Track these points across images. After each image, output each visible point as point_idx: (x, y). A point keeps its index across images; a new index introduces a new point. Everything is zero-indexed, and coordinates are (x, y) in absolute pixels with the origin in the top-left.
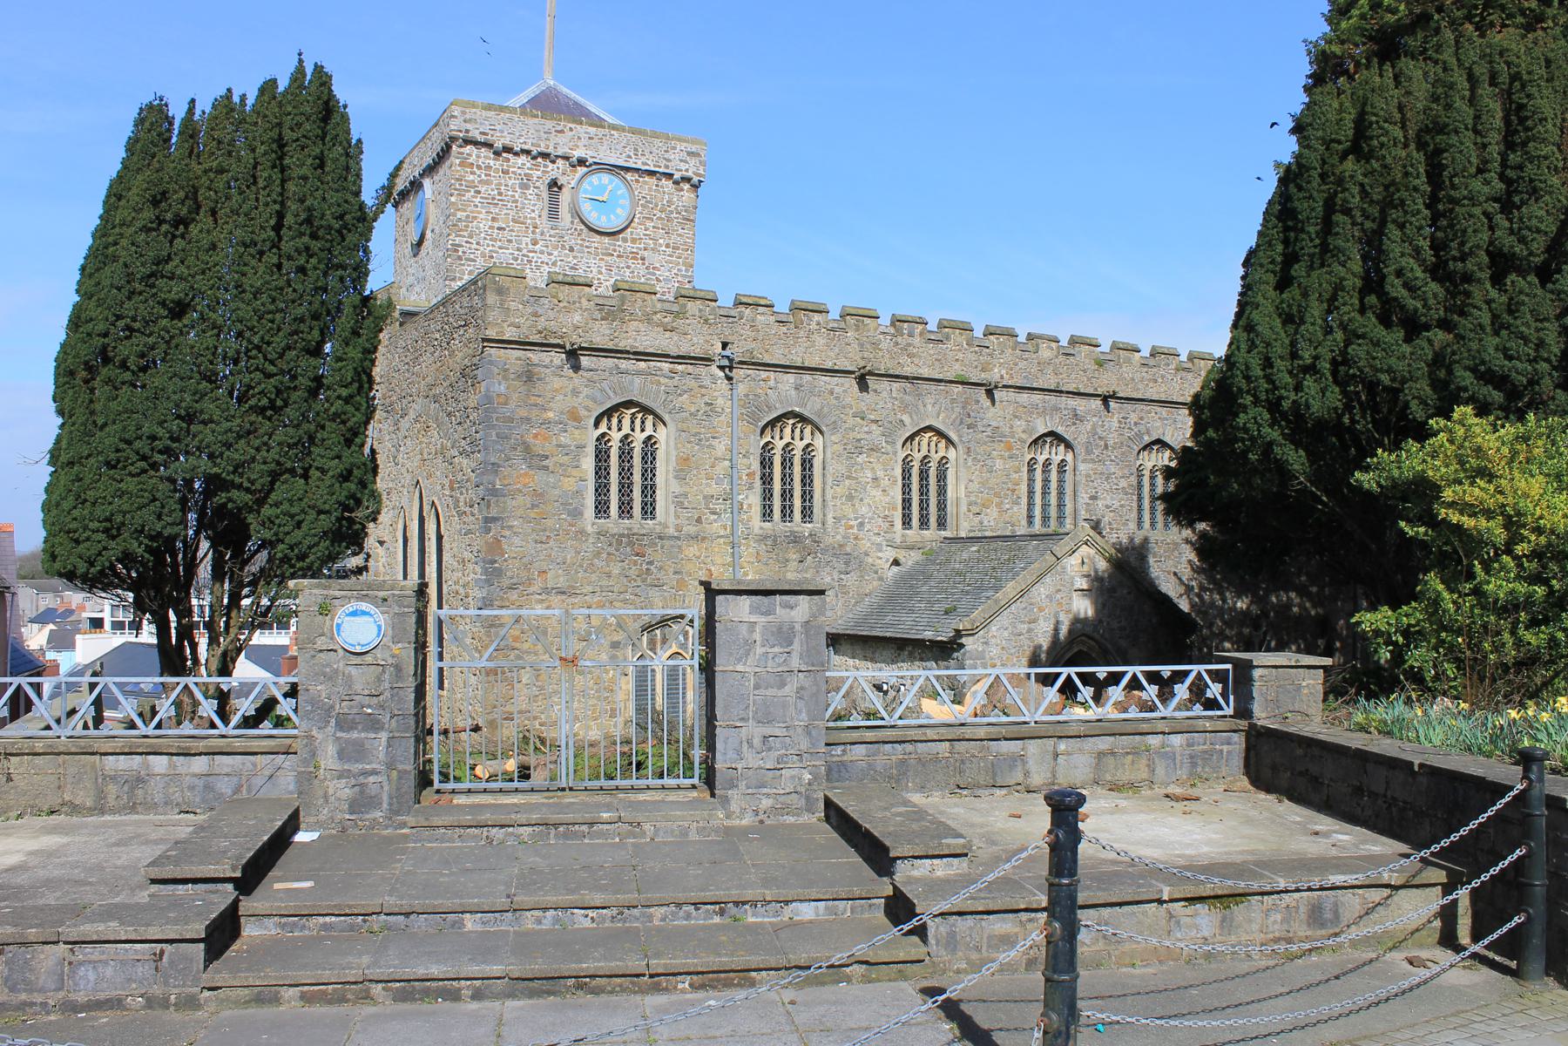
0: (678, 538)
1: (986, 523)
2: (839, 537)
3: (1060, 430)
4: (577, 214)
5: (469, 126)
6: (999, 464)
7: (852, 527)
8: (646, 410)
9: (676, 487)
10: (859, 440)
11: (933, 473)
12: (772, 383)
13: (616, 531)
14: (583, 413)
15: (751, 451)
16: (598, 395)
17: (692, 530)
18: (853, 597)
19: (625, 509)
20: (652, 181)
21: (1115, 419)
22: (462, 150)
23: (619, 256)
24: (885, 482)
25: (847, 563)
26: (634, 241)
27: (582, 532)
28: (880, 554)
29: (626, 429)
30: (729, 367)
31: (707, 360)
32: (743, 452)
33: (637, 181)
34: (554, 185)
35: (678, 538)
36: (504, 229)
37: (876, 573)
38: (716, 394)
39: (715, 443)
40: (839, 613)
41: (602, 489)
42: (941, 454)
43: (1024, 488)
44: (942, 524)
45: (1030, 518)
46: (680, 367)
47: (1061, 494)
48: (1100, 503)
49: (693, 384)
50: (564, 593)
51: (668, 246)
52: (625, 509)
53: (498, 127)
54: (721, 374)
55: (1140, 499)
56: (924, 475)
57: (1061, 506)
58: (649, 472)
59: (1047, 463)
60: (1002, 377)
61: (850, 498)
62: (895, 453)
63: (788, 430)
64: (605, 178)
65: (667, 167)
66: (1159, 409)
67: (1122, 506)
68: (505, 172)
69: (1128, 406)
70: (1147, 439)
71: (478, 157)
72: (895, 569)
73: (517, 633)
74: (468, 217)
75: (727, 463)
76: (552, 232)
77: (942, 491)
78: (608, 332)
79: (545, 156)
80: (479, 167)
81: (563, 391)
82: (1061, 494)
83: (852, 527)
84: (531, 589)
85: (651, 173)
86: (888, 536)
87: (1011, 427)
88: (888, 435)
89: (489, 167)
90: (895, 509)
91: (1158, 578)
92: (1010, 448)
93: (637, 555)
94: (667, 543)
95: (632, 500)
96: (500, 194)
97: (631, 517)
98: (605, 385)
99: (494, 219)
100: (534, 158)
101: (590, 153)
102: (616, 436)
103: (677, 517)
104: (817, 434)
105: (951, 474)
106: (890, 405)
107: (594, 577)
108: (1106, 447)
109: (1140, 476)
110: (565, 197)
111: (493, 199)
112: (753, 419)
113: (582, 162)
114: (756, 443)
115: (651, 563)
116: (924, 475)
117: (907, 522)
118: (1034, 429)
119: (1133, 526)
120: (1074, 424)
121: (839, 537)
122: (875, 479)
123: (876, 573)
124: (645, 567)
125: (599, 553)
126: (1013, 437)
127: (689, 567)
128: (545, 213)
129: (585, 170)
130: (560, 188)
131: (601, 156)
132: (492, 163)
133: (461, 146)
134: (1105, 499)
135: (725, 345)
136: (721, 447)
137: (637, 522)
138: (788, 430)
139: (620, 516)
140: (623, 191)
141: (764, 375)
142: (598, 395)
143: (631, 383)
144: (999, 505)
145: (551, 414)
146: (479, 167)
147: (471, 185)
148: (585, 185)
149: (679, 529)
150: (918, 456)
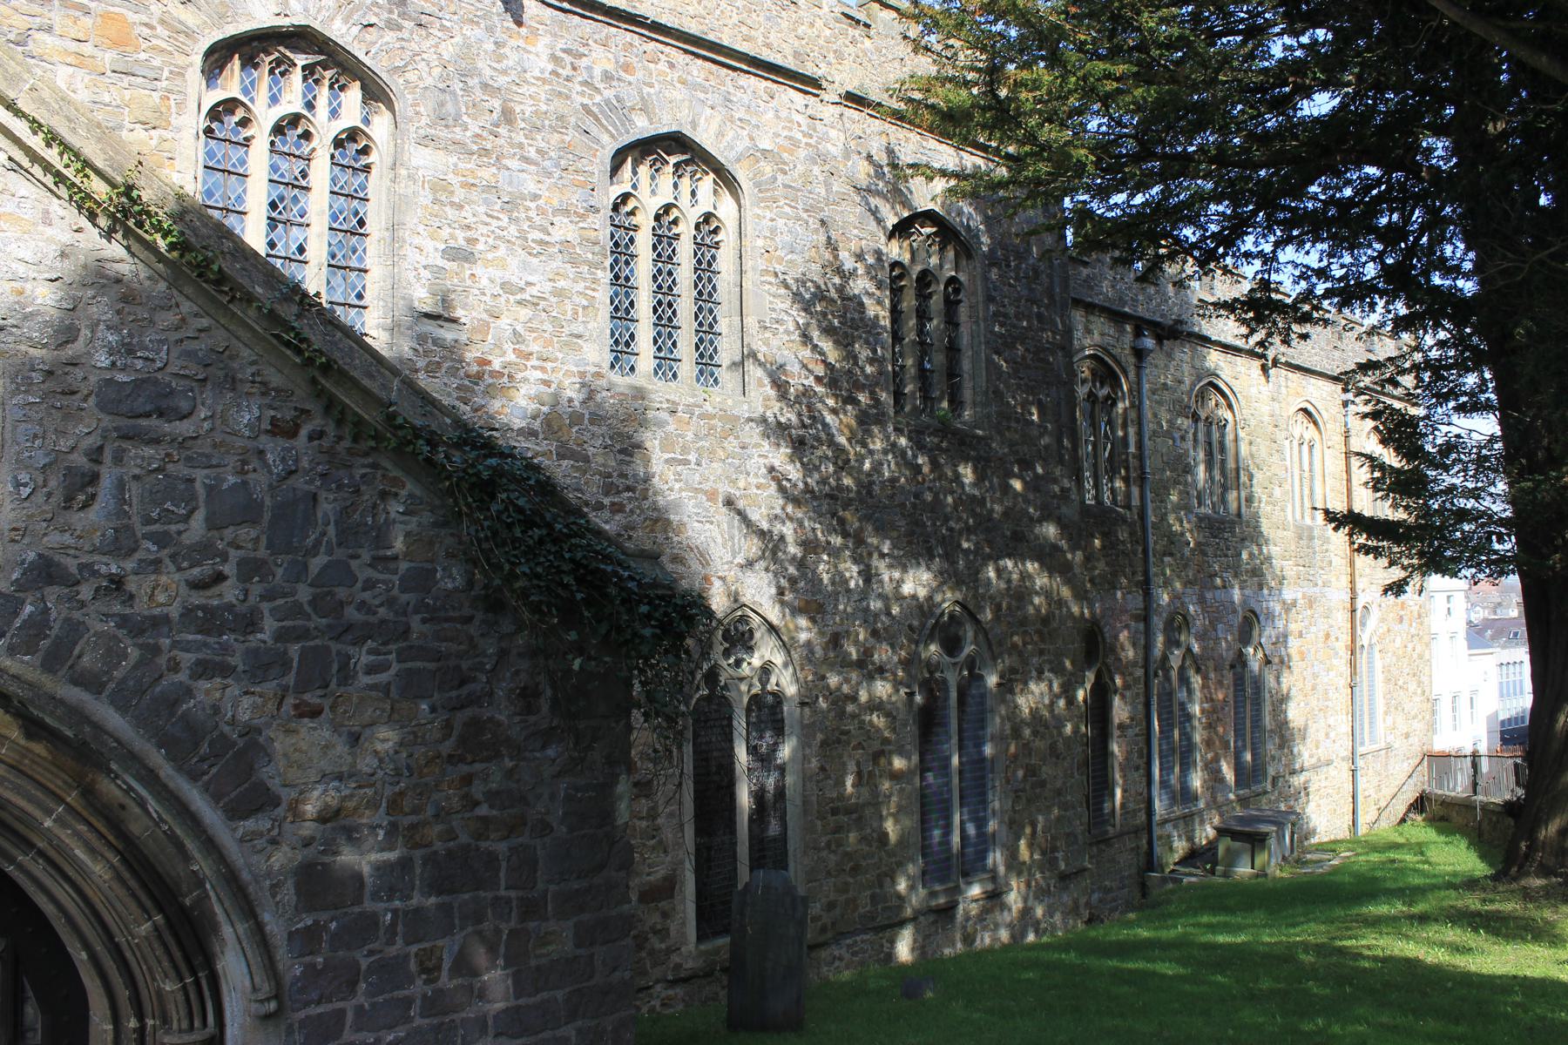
21: (542, 46)
55: (621, 281)
67: (559, 293)
70: (643, 127)
91: (677, 505)
92: (120, 43)
108: (508, 116)
119: (596, 353)
120: (393, 26)
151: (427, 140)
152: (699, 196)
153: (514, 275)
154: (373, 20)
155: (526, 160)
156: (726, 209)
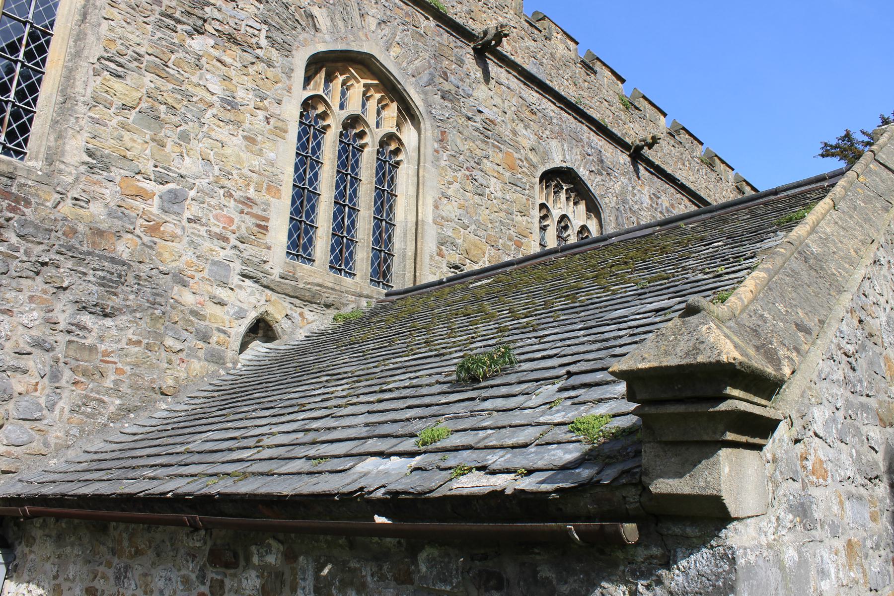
2: (96, 209)
3: (583, 172)
6: (494, 186)
7: (142, 195)
18: (116, 390)
25: (110, 284)
28: (222, 293)
37: (205, 338)
40: (55, 435)
72: (258, 348)
83: (142, 195)
86: (249, 251)
118: (545, 156)
123: (205, 338)
154: (593, 169)
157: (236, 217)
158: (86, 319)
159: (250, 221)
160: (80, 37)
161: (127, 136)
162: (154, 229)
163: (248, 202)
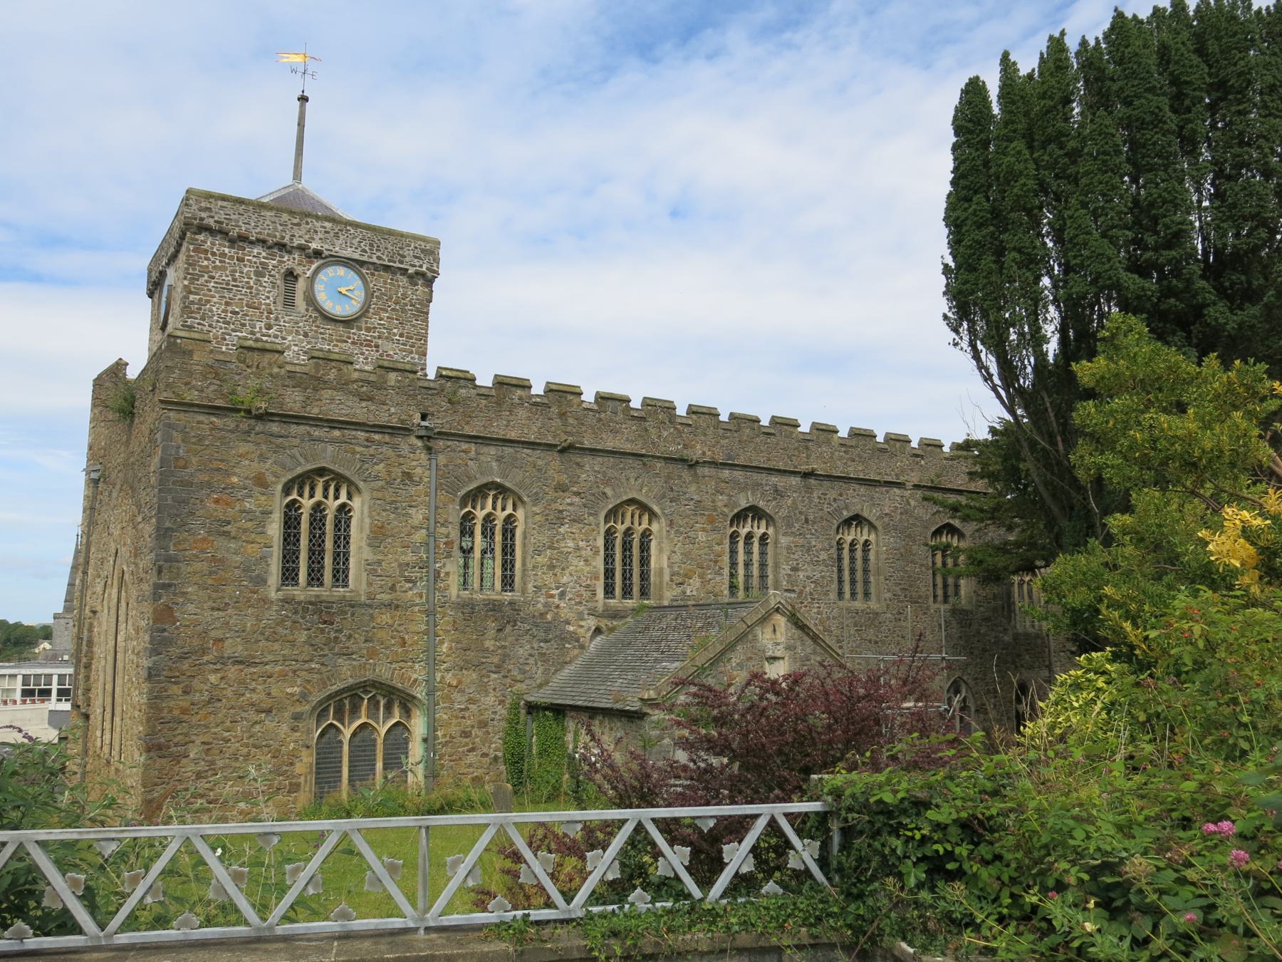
0: (370, 606)
1: (688, 593)
3: (761, 504)
4: (311, 300)
5: (204, 215)
6: (702, 537)
7: (552, 596)
8: (340, 479)
9: (368, 554)
10: (561, 512)
11: (636, 544)
12: (472, 454)
13: (302, 598)
14: (270, 478)
15: (450, 520)
16: (288, 462)
17: (385, 597)
19: (315, 577)
20: (388, 277)
22: (197, 237)
23: (353, 343)
24: (587, 553)
26: (368, 330)
27: (265, 600)
28: (582, 623)
29: (319, 496)
30: (428, 438)
31: (404, 431)
32: (442, 521)
33: (373, 274)
34: (291, 276)
35: (370, 606)
36: (237, 313)
37: (578, 641)
38: (414, 463)
39: (412, 511)
41: (289, 557)
42: (645, 525)
43: (726, 558)
44: (644, 593)
45: (733, 587)
46: (377, 437)
47: (763, 565)
48: (801, 574)
49: (390, 453)
50: (240, 662)
51: (401, 335)
52: (315, 577)
53: (233, 217)
54: (419, 443)
55: (840, 570)
56: (627, 546)
57: (763, 577)
58: (342, 539)
59: (749, 536)
60: (704, 453)
61: (552, 567)
62: (598, 525)
63: (490, 501)
64: (341, 271)
65: (401, 262)
66: (857, 487)
67: (823, 577)
68: (240, 260)
69: (826, 484)
70: (846, 514)
71: (213, 244)
73: (185, 704)
74: (200, 300)
75: (424, 531)
76: (287, 318)
77: (645, 561)
78: (301, 398)
79: (282, 246)
80: (214, 254)
81: (249, 457)
82: (763, 565)
84: (205, 658)
85: (387, 268)
86: (590, 605)
87: (713, 501)
88: (591, 507)
89: (223, 255)
90: (597, 578)
93: (325, 622)
94: (359, 611)
95: (323, 567)
96: (235, 280)
97: (322, 584)
98: (295, 451)
99: (227, 304)
100: (270, 248)
101: (326, 246)
102: (307, 503)
103: (370, 584)
104: (519, 503)
105: (653, 545)
106: (592, 478)
107: (276, 646)
108: (807, 521)
109: (840, 549)
110: (301, 285)
111: (228, 284)
112: (453, 490)
113: (318, 254)
114: (454, 513)
115: (340, 631)
116: (627, 546)
117: (609, 591)
118: (736, 504)
120: (775, 499)
121: (539, 606)
122: (578, 549)
124: (333, 635)
125: (283, 621)
126: (715, 510)
127: (381, 634)
128: (281, 299)
129: (321, 262)
130: (296, 278)
131: (337, 249)
132: (227, 250)
133: (195, 233)
134: (806, 570)
135: (424, 417)
136: (417, 516)
137: (327, 591)
138: (490, 501)
139: (309, 584)
140: (358, 283)
141: (464, 446)
142: (288, 462)
143: (324, 450)
144: (701, 576)
145: (235, 479)
146: (214, 254)
147: (205, 270)
148: (321, 276)
149: (371, 596)
150: (621, 528)
151: (785, 534)
152: (864, 535)
153: (809, 574)
155: (812, 534)
156: (872, 538)
157: (584, 593)
158: (542, 644)
159: (589, 593)
160: (524, 545)
161: (544, 577)
162: (558, 607)
163: (588, 586)
